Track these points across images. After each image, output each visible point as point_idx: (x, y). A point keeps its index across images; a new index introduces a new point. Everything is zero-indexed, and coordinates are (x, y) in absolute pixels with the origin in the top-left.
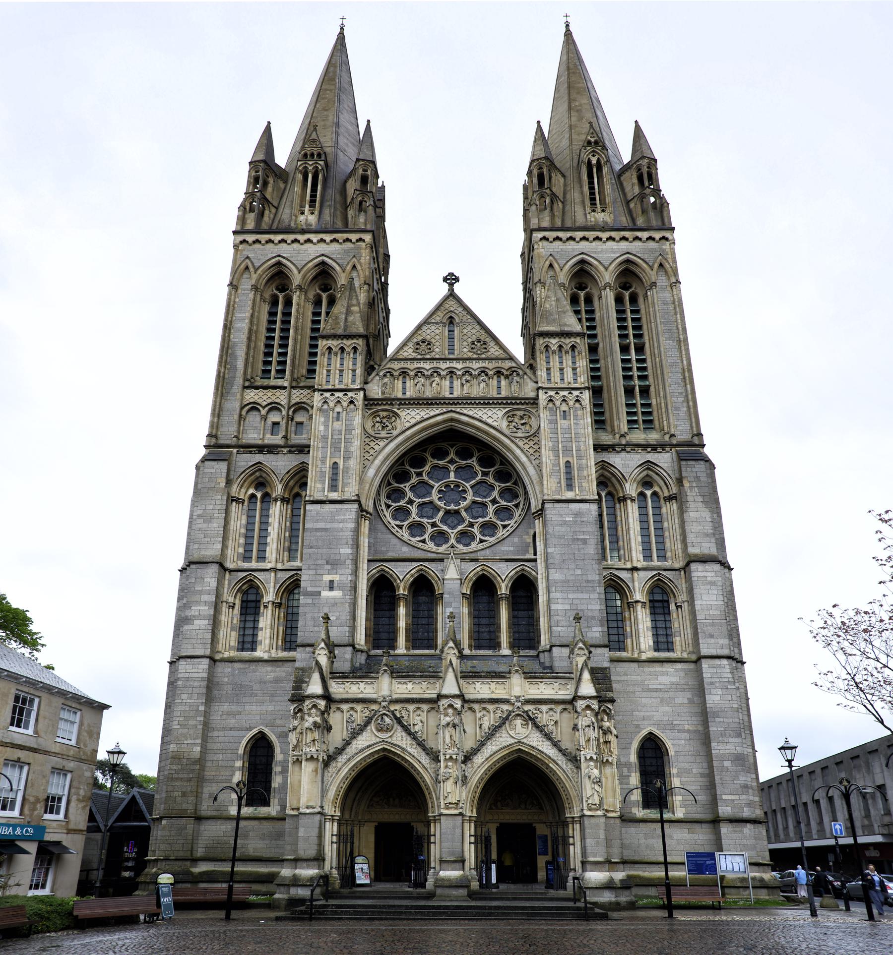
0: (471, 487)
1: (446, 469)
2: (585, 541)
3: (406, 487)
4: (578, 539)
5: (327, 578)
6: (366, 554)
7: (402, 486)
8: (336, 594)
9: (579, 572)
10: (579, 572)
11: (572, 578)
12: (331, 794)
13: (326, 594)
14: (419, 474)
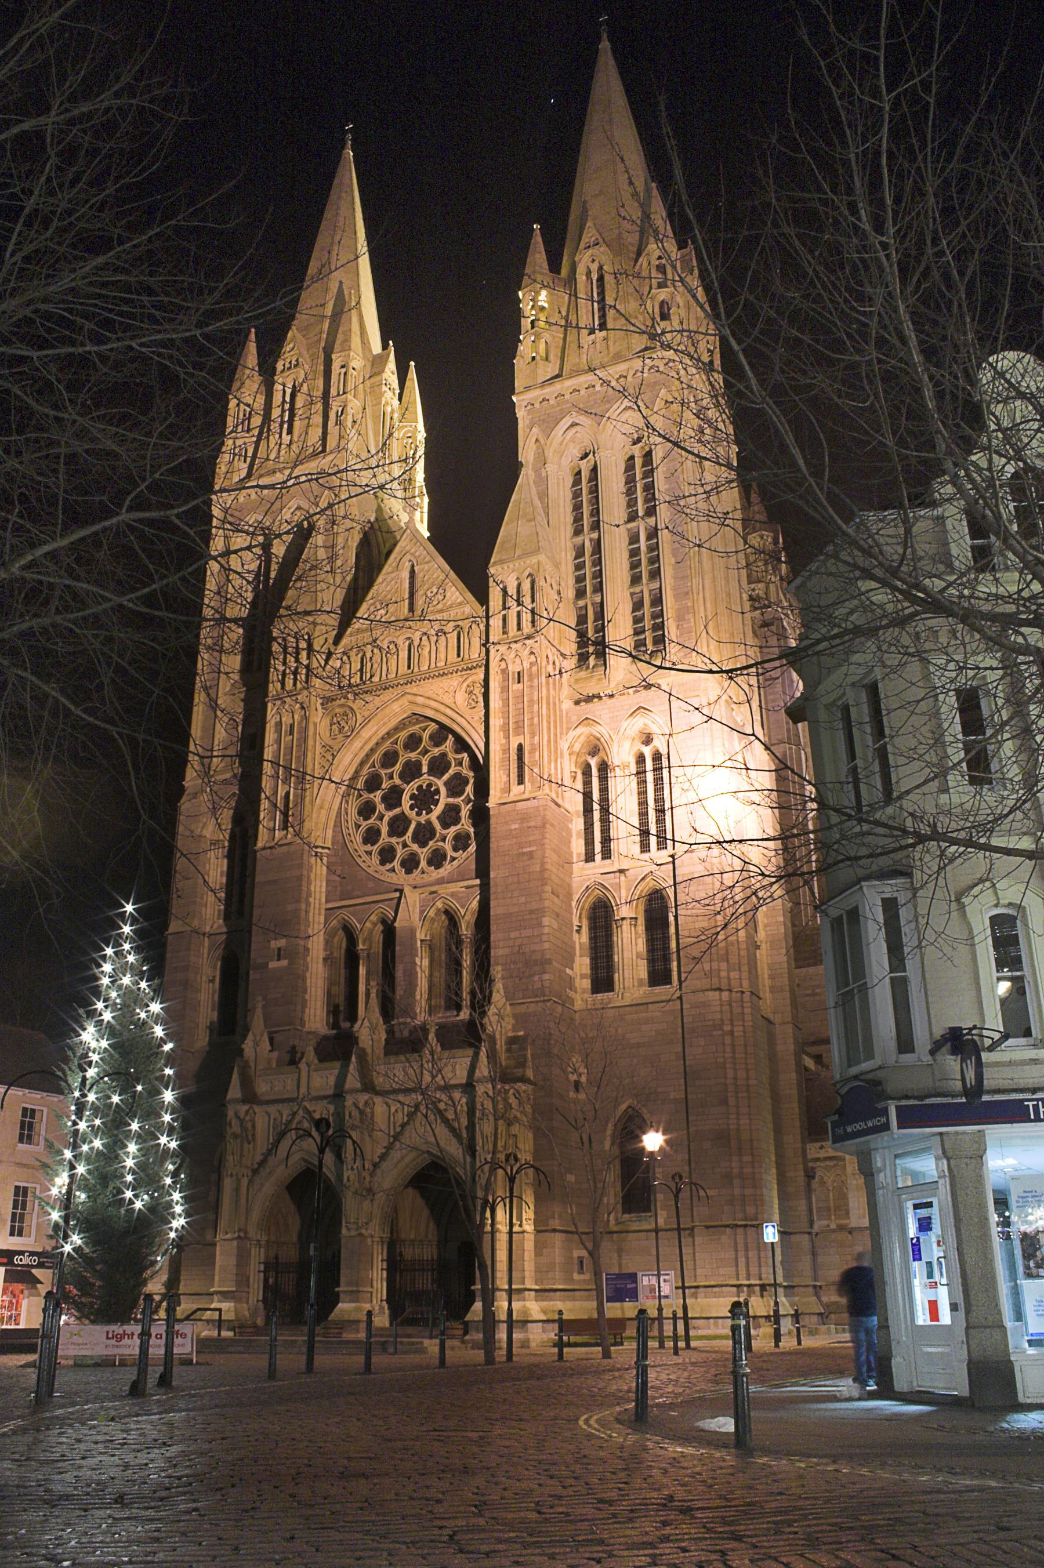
0: (446, 784)
1: (418, 764)
2: (531, 855)
3: (377, 796)
4: (524, 854)
5: (275, 944)
6: (323, 900)
7: (372, 796)
8: (284, 963)
9: (522, 900)
10: (522, 900)
11: (516, 909)
12: (255, 1215)
13: (272, 965)
14: (391, 777)
